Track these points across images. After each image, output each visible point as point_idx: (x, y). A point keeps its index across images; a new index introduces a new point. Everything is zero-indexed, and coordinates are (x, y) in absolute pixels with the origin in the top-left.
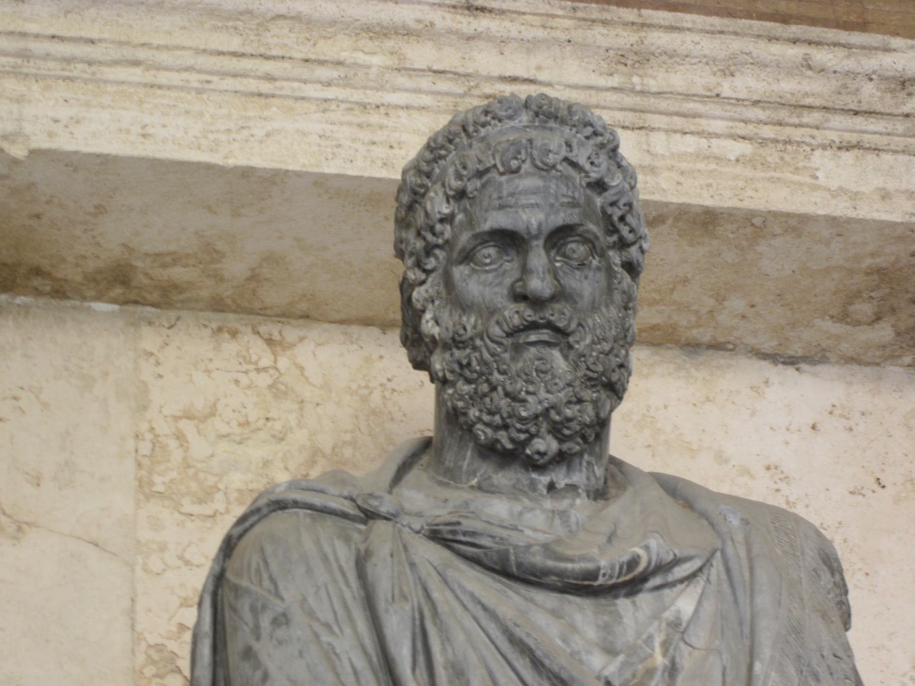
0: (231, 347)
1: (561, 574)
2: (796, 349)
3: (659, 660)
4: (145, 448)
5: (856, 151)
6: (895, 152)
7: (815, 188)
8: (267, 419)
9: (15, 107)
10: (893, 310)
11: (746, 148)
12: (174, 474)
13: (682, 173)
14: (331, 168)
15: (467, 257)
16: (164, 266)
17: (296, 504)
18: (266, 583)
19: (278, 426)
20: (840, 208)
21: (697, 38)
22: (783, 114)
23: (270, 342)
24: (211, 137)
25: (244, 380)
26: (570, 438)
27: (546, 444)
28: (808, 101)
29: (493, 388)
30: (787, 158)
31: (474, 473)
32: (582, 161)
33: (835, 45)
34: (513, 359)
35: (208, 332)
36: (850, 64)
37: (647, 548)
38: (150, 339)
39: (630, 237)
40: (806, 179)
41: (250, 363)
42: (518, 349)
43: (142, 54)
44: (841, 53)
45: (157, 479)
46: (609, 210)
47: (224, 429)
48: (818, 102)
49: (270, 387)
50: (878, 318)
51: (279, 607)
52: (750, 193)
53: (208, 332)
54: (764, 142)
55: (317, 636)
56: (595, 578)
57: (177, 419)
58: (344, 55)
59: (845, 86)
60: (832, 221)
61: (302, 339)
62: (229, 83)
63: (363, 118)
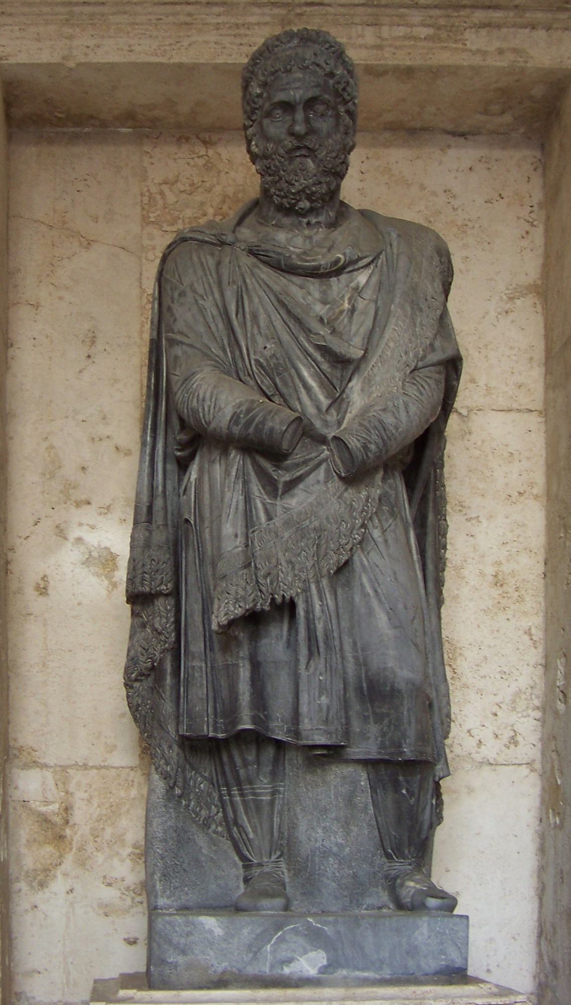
5: (487, 29)
8: (203, 181)
27: (305, 204)
31: (273, 218)
34: (290, 164)
41: (195, 153)
47: (183, 188)
49: (205, 165)
61: (220, 139)
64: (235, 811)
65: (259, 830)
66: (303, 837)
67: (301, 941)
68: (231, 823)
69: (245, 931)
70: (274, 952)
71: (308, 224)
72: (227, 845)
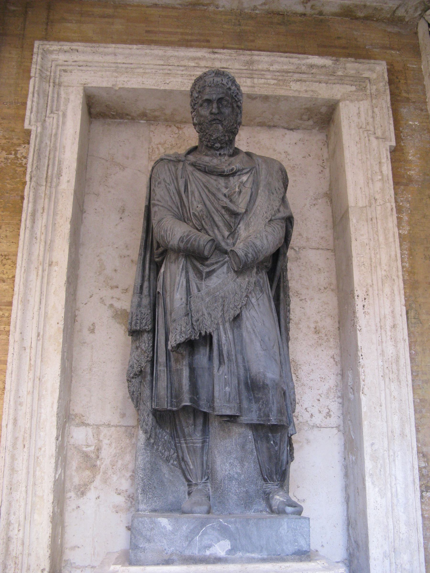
0: (170, 129)
1: (217, 172)
2: (292, 127)
3: (237, 190)
4: (151, 151)
6: (309, 82)
7: (290, 90)
9: (115, 79)
10: (312, 118)
11: (275, 82)
12: (156, 156)
13: (261, 87)
14: (183, 89)
15: (201, 105)
16: (153, 112)
17: (165, 159)
18: (157, 175)
19: (179, 145)
20: (296, 94)
21: (264, 57)
22: (284, 74)
23: (178, 128)
24: (157, 83)
25: (172, 136)
26: (223, 144)
28: (289, 71)
29: (207, 133)
30: (285, 83)
32: (225, 83)
33: (296, 58)
35: (165, 126)
36: (299, 62)
37: (236, 166)
38: (152, 128)
39: (238, 100)
40: (289, 88)
42: (211, 125)
43: (142, 66)
44: (297, 60)
45: (153, 157)
46: (232, 94)
47: (167, 146)
48: (292, 71)
50: (309, 119)
51: (159, 180)
52: (275, 91)
53: (165, 126)
54: (279, 80)
55: (166, 186)
56: (224, 172)
57: (157, 144)
58: (186, 64)
59: (298, 67)
60: (294, 97)
62: (161, 71)
63: (190, 78)
64: (183, 453)
65: (196, 464)
66: (219, 469)
67: (216, 534)
68: (181, 459)
69: (184, 528)
70: (201, 540)
71: (220, 154)
72: (179, 473)
